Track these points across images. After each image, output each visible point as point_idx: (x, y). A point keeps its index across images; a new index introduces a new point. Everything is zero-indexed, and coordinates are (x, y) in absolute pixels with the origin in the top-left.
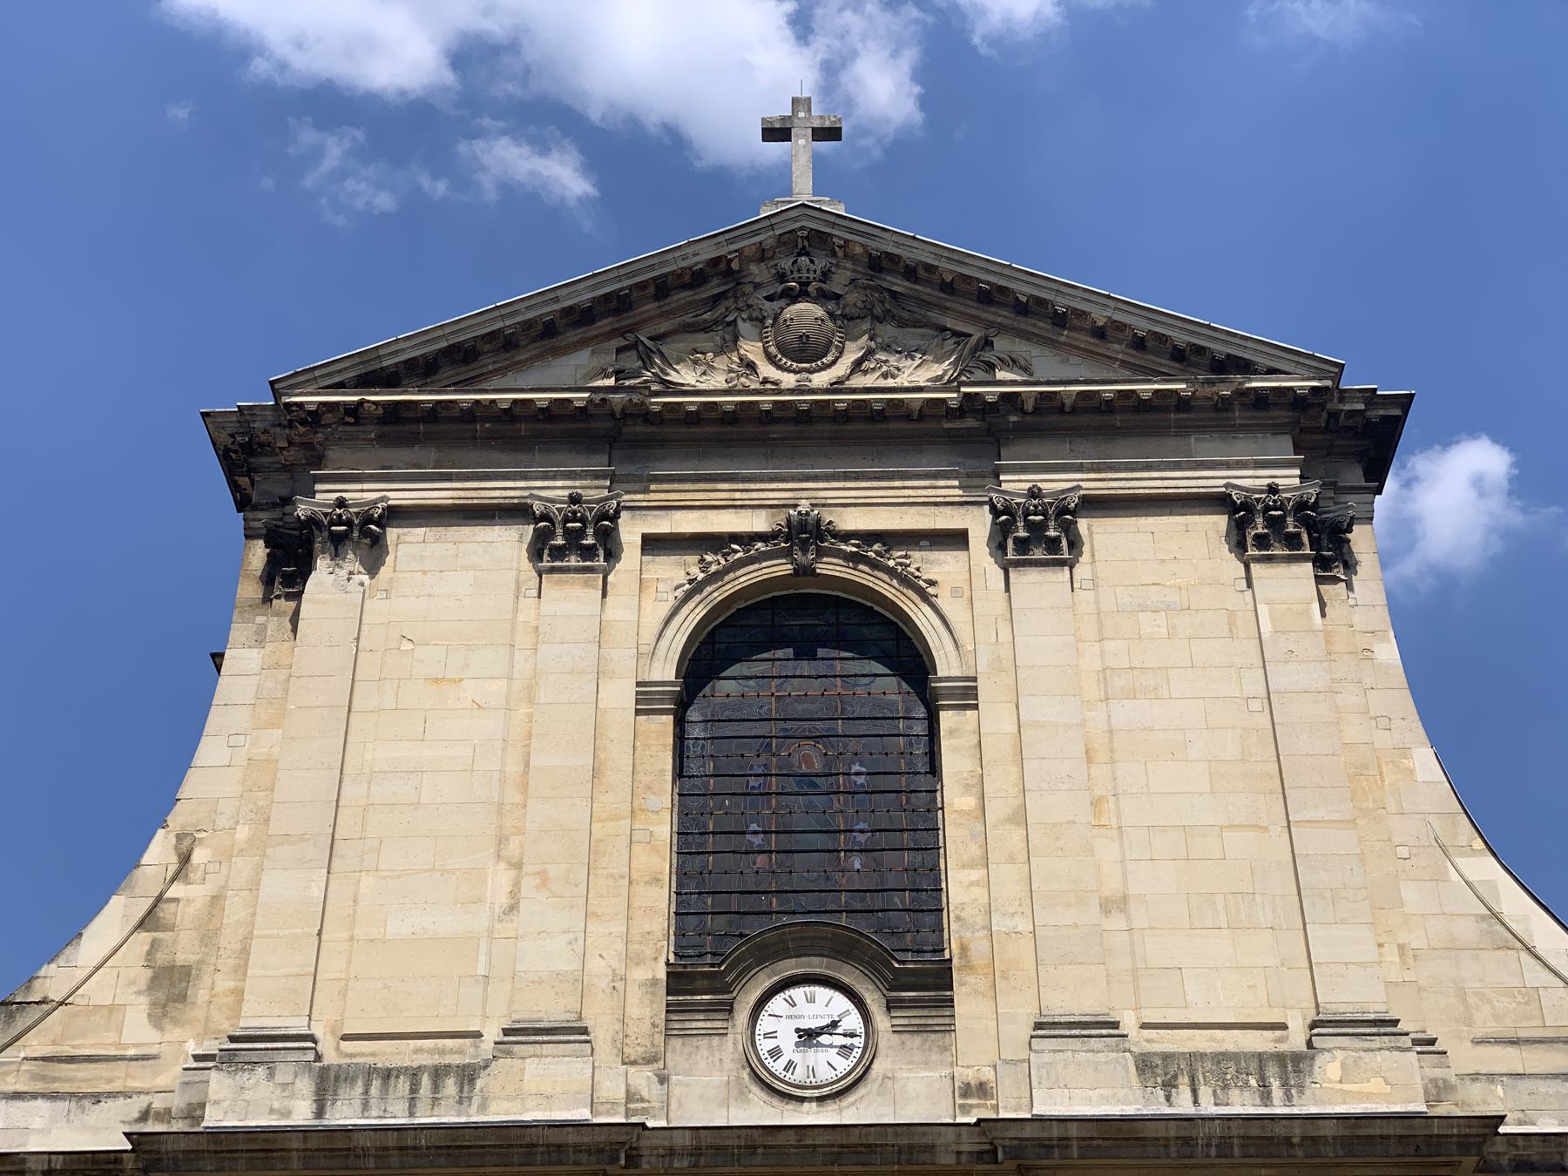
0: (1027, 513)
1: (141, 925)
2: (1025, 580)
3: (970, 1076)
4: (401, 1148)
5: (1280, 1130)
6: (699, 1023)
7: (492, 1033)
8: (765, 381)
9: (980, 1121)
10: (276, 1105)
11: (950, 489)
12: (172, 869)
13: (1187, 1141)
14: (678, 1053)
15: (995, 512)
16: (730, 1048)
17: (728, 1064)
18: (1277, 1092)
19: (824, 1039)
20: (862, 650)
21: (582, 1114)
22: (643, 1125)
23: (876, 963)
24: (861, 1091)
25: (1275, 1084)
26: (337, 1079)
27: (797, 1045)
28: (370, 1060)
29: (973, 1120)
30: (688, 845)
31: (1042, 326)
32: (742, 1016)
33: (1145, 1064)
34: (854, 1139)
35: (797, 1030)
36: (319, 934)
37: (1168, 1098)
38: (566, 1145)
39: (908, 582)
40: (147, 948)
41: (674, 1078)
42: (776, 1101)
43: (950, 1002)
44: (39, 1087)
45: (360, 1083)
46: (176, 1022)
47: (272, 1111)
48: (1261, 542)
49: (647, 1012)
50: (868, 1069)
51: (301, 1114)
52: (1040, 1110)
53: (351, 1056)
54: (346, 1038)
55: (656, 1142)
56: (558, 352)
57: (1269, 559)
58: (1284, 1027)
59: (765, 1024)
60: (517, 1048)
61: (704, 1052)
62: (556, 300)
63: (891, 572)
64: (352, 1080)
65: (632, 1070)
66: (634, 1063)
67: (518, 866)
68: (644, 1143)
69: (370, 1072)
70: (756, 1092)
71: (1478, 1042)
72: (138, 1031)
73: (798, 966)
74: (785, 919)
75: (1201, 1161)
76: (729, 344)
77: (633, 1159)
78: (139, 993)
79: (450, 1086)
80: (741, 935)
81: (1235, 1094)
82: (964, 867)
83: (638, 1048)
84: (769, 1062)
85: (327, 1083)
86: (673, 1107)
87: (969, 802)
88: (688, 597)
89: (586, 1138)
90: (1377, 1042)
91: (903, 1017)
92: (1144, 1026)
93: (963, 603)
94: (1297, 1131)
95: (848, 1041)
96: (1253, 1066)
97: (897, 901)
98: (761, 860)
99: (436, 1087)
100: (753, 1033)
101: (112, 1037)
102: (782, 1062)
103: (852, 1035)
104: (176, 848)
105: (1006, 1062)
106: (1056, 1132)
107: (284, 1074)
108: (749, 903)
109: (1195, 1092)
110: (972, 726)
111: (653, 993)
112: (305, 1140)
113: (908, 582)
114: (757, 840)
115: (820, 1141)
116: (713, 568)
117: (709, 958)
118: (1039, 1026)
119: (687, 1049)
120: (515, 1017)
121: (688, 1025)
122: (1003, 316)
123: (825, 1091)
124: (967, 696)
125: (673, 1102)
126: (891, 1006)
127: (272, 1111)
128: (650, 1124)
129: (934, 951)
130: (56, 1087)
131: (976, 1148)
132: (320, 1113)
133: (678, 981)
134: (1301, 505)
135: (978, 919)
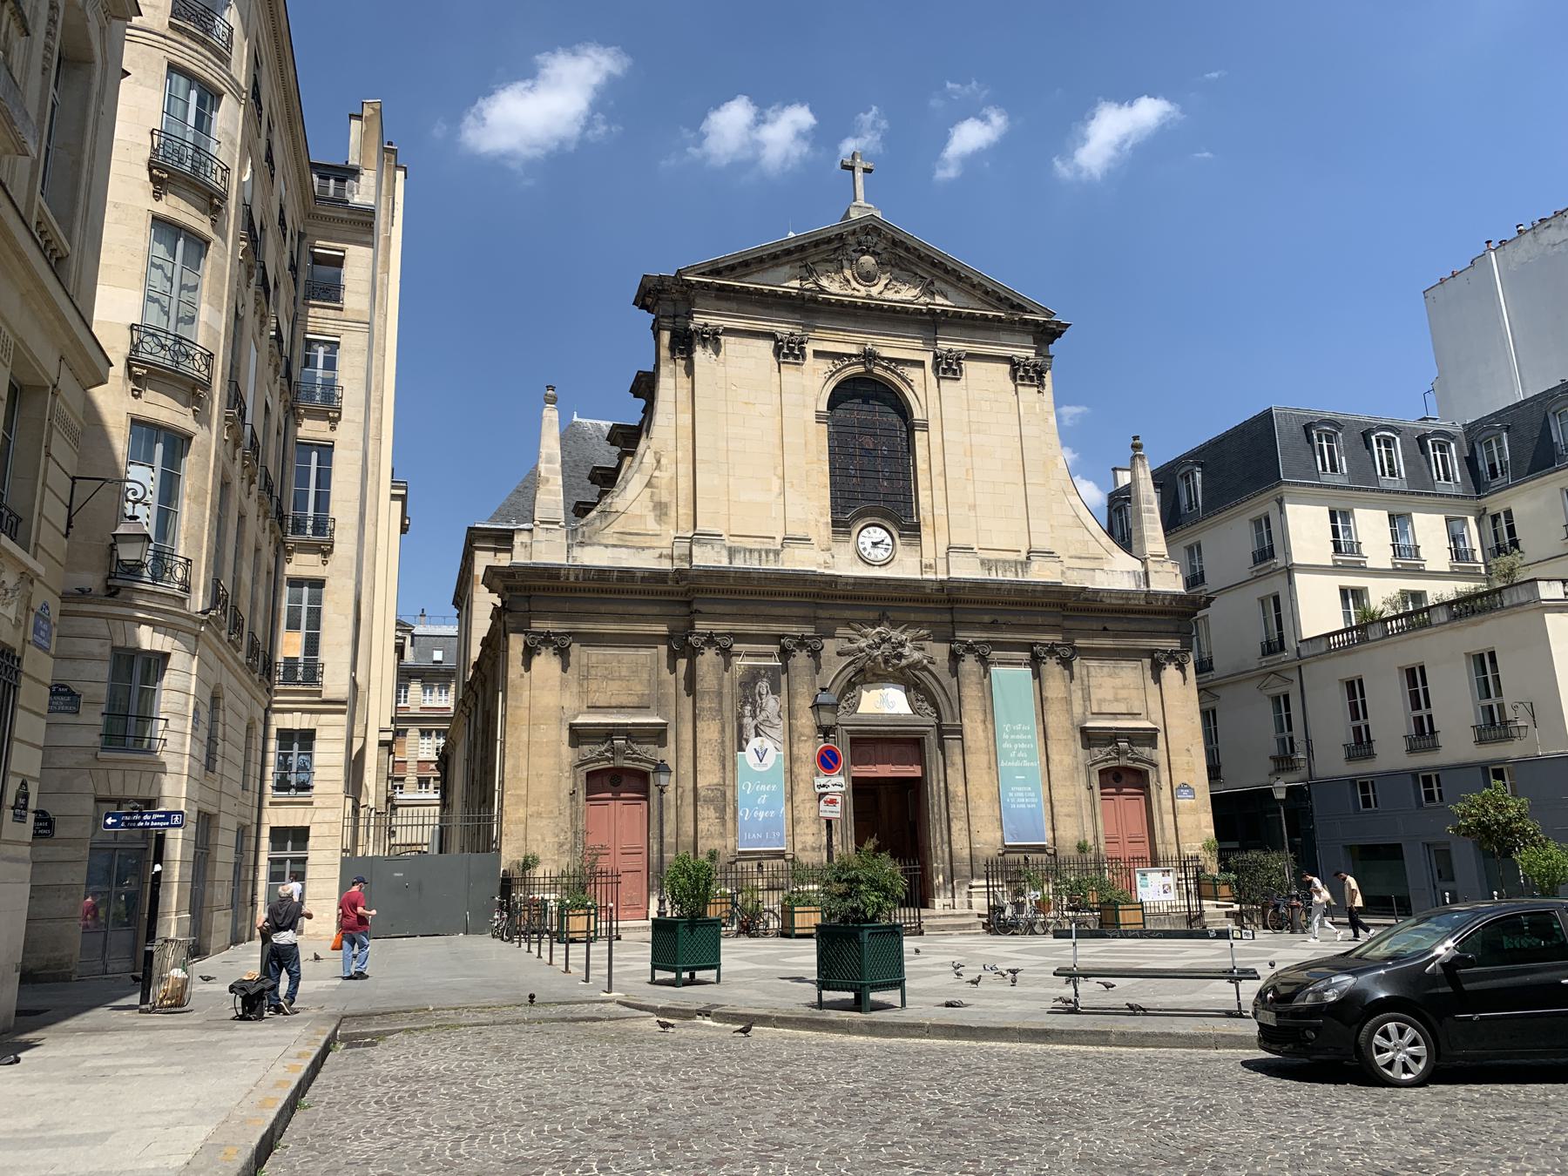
0: (947, 358)
1: (646, 486)
6: (841, 538)
8: (854, 289)
11: (919, 344)
14: (835, 548)
16: (851, 547)
18: (1020, 574)
20: (884, 401)
23: (897, 522)
25: (1020, 571)
39: (904, 379)
44: (620, 543)
46: (665, 523)
48: (1022, 378)
49: (826, 533)
51: (725, 562)
57: (1024, 385)
59: (861, 539)
63: (899, 375)
64: (740, 552)
69: (745, 549)
71: (1071, 557)
72: (651, 525)
76: (840, 269)
79: (771, 556)
85: (732, 552)
88: (830, 377)
90: (1049, 559)
91: (904, 540)
99: (767, 556)
101: (643, 527)
113: (904, 379)
116: (838, 367)
124: (925, 426)
130: (627, 543)
133: (835, 523)
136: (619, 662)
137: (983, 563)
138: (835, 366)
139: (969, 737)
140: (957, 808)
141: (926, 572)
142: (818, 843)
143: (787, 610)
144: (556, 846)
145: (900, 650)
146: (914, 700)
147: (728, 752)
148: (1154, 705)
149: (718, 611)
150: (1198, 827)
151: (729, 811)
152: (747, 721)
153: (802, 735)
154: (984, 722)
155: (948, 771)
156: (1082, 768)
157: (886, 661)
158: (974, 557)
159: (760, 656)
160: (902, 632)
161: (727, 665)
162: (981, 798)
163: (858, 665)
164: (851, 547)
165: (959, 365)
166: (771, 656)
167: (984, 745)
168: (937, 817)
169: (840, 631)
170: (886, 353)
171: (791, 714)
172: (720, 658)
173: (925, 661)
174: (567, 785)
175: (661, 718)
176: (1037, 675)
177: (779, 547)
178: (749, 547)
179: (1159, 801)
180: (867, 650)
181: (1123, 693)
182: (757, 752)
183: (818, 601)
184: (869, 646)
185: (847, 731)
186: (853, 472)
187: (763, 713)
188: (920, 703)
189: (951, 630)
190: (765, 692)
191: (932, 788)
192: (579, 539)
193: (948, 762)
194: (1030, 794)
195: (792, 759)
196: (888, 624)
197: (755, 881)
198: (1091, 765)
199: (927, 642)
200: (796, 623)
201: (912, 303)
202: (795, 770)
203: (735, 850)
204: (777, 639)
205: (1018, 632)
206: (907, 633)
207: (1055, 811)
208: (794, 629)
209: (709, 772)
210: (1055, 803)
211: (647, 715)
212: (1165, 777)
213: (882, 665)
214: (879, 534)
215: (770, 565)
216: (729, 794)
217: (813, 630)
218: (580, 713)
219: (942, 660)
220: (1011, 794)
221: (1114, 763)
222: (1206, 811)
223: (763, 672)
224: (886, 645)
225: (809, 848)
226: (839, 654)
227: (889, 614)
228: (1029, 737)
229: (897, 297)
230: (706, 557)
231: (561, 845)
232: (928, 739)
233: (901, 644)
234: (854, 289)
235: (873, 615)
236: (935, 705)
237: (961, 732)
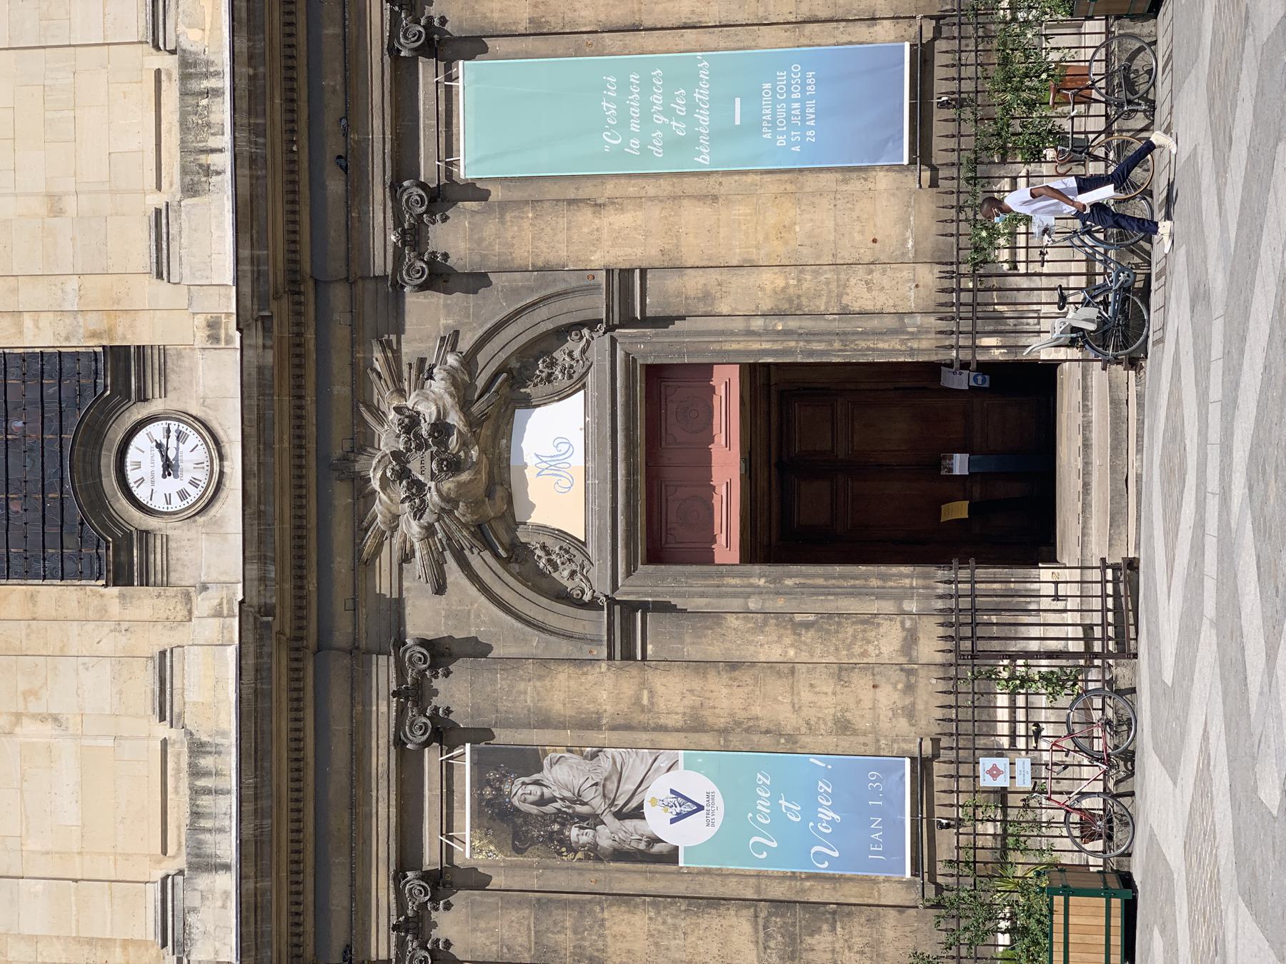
3: (202, 334)
4: (256, 799)
5: (243, 84)
6: (157, 558)
7: (164, 730)
9: (238, 329)
10: (219, 903)
13: (253, 161)
14: (183, 575)
17: (192, 534)
19: (171, 455)
21: (231, 653)
22: (241, 603)
23: (105, 411)
24: (215, 425)
25: (205, 84)
26: (198, 856)
27: (176, 477)
28: (184, 829)
29: (238, 334)
33: (191, 190)
34: (254, 431)
35: (164, 476)
36: (76, 881)
37: (218, 173)
38: (256, 664)
41: (203, 579)
42: (223, 495)
45: (202, 837)
47: (224, 907)
49: (147, 602)
52: (229, 277)
54: (164, 852)
55: (254, 593)
58: (158, 72)
59: (158, 504)
60: (176, 710)
61: (182, 554)
64: (200, 843)
65: (196, 613)
66: (190, 612)
68: (255, 602)
69: (194, 829)
70: (215, 511)
73: (109, 476)
74: (68, 486)
75: (269, 151)
77: (267, 610)
79: (206, 762)
80: (82, 524)
81: (214, 118)
82: (21, 332)
83: (178, 609)
84: (191, 500)
85: (202, 863)
86: (227, 579)
89: (251, 649)
91: (153, 387)
92: (159, 187)
94: (244, 70)
95: (173, 435)
96: (191, 100)
97: (51, 391)
100: (166, 513)
102: (191, 489)
103: (168, 431)
105: (190, 305)
106: (246, 267)
107: (193, 900)
108: (53, 517)
109: (213, 151)
111: (132, 597)
112: (247, 877)
115: (254, 459)
117: (102, 551)
118: (159, 275)
119: (179, 568)
120: (150, 712)
121: (159, 568)
123: (215, 454)
125: (222, 579)
127: (224, 907)
128: (240, 597)
129: (96, 360)
131: (260, 333)
132: (226, 867)
133: (121, 576)
135: (67, 321)
137: (191, 190)
139: (639, 251)
142: (896, 675)
145: (424, 429)
146: (548, 388)
147: (680, 888)
149: (346, 903)
151: (818, 894)
152: (606, 835)
153: (637, 701)
154: (598, 206)
157: (454, 466)
158: (179, 212)
159: (450, 792)
160: (380, 417)
161: (477, 881)
162: (789, 228)
163: (465, 543)
166: (450, 767)
167: (656, 212)
168: (837, 345)
169: (384, 584)
171: (590, 723)
172: (459, 898)
176: (474, 46)
178: (186, 820)
180: (428, 518)
182: (680, 817)
183: (312, 640)
184: (418, 513)
185: (629, 573)
187: (588, 795)
188: (557, 372)
189: (370, 285)
190: (536, 790)
193: (701, 309)
194: (782, 84)
195: (695, 726)
196: (362, 459)
197: (982, 856)
199: (405, 349)
200: (367, 703)
202: (721, 722)
203: (909, 884)
204: (408, 764)
205: (367, 93)
206: (384, 407)
207: (822, 14)
208: (383, 710)
209: (724, 944)
210: (804, 11)
213: (465, 477)
216: (778, 891)
217: (383, 659)
219: (449, 310)
220: (781, 141)
223: (488, 792)
224: (414, 466)
225: (907, 701)
226: (440, 589)
227: (338, 453)
228: (634, 78)
232: (644, 356)
233: (411, 423)
235: (341, 496)
236: (562, 333)
237: (626, 274)
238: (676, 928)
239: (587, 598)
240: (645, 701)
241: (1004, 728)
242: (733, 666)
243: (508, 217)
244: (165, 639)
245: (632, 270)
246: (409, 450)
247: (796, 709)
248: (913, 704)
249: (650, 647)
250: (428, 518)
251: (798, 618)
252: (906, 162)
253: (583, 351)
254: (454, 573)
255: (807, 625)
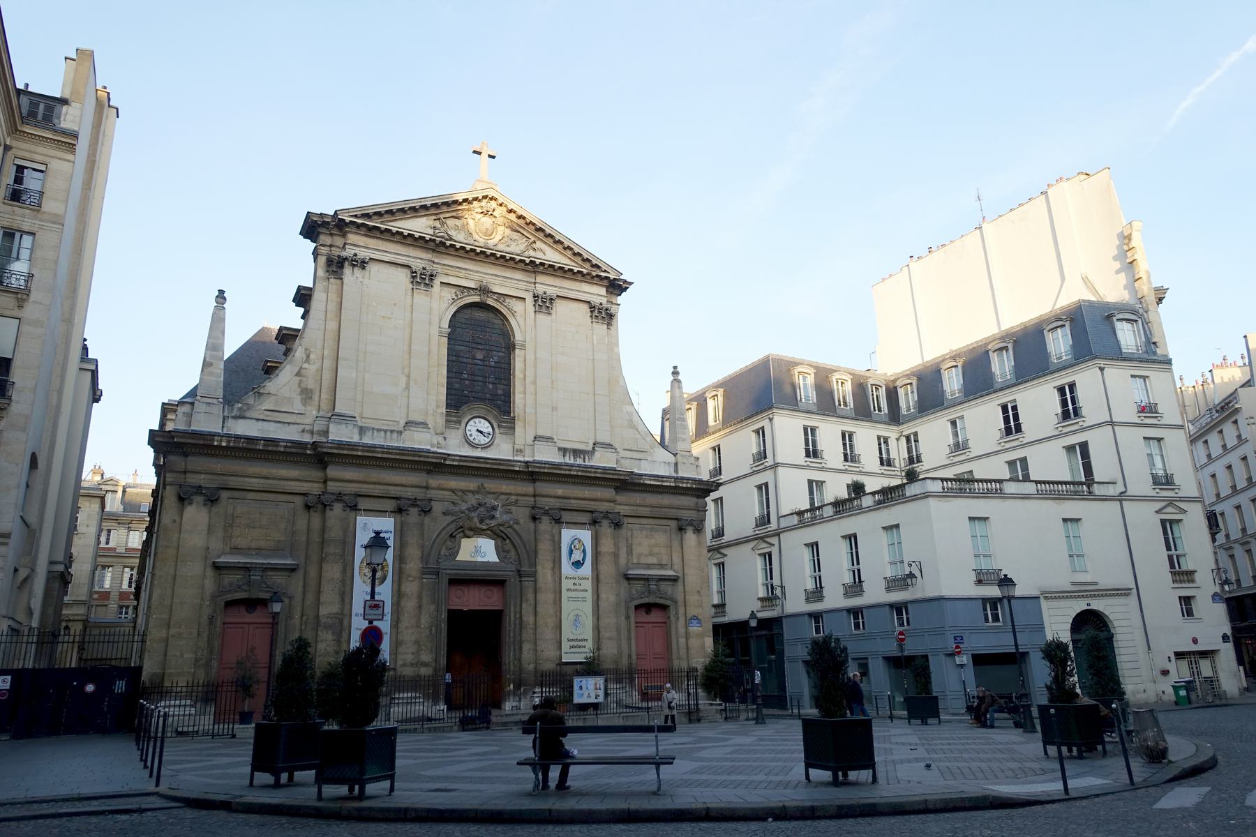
0: (542, 298)
2: (541, 317)
6: (453, 425)
7: (402, 423)
8: (475, 240)
11: (523, 285)
12: (305, 359)
14: (449, 433)
15: (535, 297)
18: (587, 460)
21: (429, 447)
24: (491, 447)
30: (450, 376)
31: (550, 241)
32: (463, 425)
33: (560, 449)
40: (298, 382)
43: (514, 428)
46: (309, 405)
49: (441, 421)
50: (493, 442)
51: (356, 439)
53: (365, 423)
54: (362, 418)
56: (417, 217)
58: (588, 443)
59: (468, 428)
62: (421, 202)
67: (409, 377)
69: (373, 429)
70: (466, 445)
71: (624, 450)
72: (298, 406)
78: (297, 395)
81: (578, 459)
84: (469, 437)
85: (362, 430)
87: (522, 376)
91: (502, 430)
93: (523, 319)
98: (467, 382)
104: (305, 353)
110: (523, 355)
114: (466, 376)
116: (460, 296)
122: (541, 235)
124: (523, 347)
126: (499, 427)
127: (348, 437)
132: (361, 439)
134: (607, 310)
136: (261, 513)
137: (560, 449)
138: (457, 296)
140: (527, 634)
141: (517, 455)
143: (404, 478)
144: (193, 661)
145: (492, 513)
146: (501, 550)
148: (676, 559)
150: (703, 647)
153: (411, 576)
154: (553, 569)
155: (524, 606)
156: (623, 604)
164: (460, 432)
165: (551, 303)
168: (512, 640)
170: (496, 289)
173: (512, 522)
174: (207, 612)
175: (293, 560)
177: (402, 429)
179: (677, 629)
180: (466, 511)
181: (656, 550)
184: (468, 509)
185: (446, 574)
186: (466, 376)
191: (510, 617)
192: (235, 412)
193: (524, 599)
198: (631, 602)
201: (518, 255)
202: (403, 603)
210: (601, 629)
211: (282, 557)
212: (681, 611)
214: (484, 426)
215: (394, 442)
216: (346, 622)
218: (224, 553)
221: (646, 600)
222: (709, 636)
224: (482, 509)
226: (444, 514)
229: (508, 249)
230: (340, 433)
231: (197, 660)
233: (494, 508)
234: (475, 240)
238: (335, 587)
239: (440, 561)
240: (410, 579)
241: (401, 695)
242: (420, 607)
243: (550, 542)
244: (430, 426)
245: (535, 577)
246: (487, 507)
247: (406, 628)
248: (407, 666)
249: (425, 580)
250: (466, 511)
251: (433, 628)
252: (563, 661)
253: (511, 562)
254: (450, 518)
255: (431, 631)
